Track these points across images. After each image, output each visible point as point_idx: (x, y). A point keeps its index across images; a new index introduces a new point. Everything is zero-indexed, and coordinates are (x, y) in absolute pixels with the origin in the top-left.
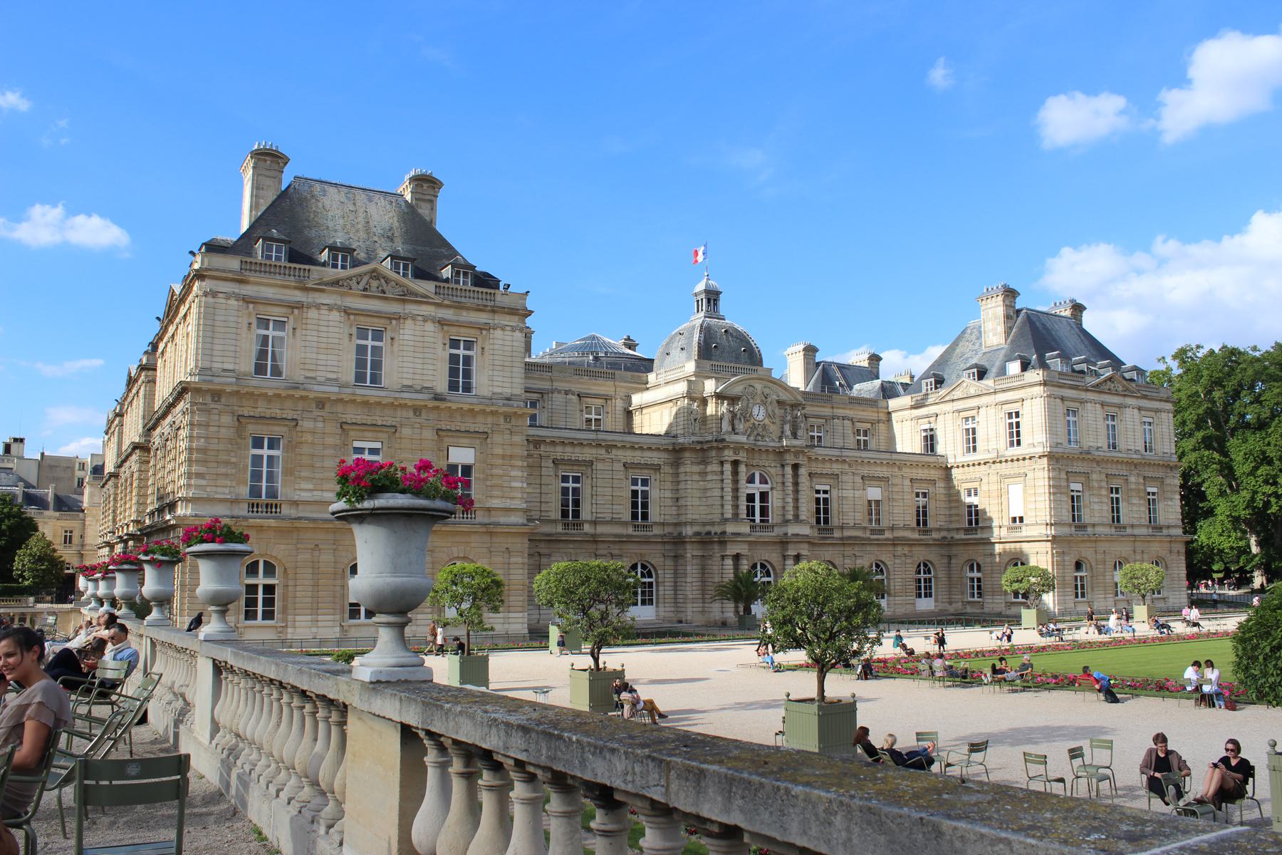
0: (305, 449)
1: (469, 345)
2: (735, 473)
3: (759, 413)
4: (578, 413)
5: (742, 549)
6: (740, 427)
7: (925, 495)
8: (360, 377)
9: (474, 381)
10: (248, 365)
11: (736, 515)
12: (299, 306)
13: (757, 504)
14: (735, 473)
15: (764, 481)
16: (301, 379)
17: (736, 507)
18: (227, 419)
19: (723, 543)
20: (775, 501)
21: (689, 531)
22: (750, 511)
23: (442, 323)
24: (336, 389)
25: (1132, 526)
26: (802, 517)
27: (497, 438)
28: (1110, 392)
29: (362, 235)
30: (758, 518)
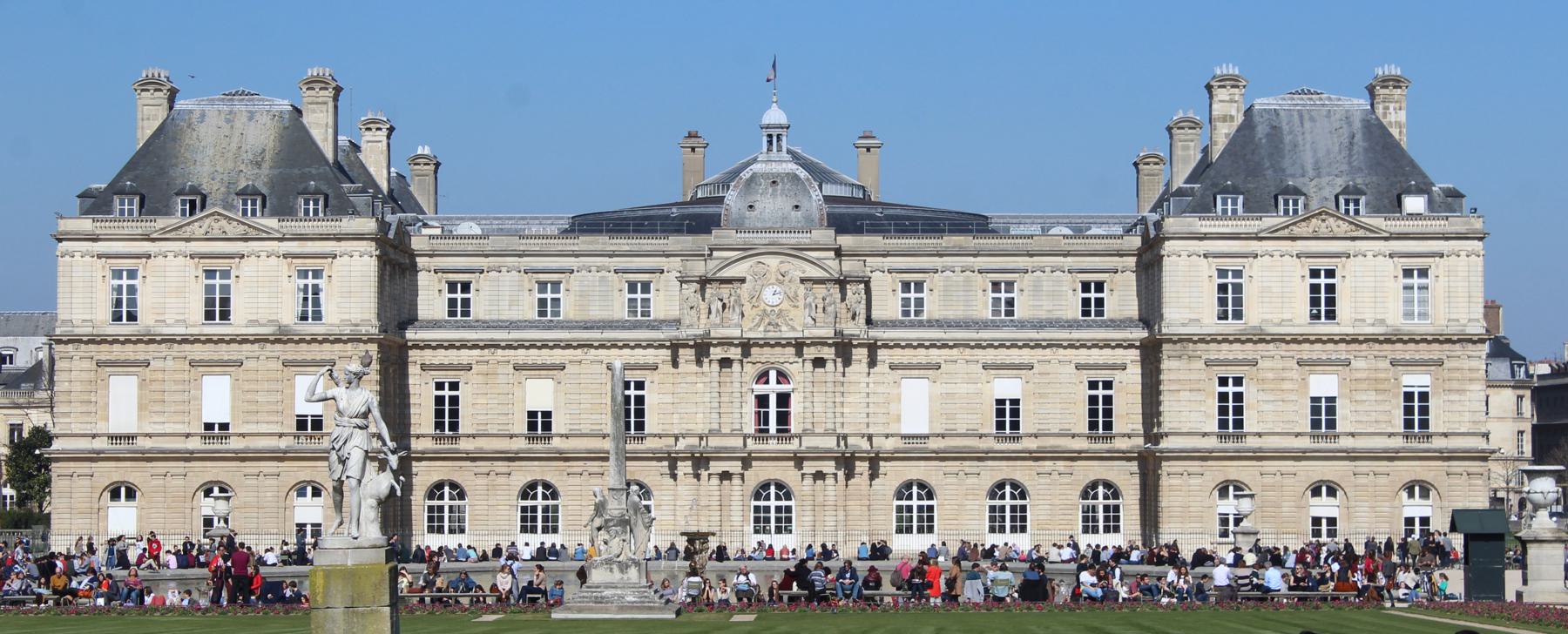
0: (156, 386)
1: (317, 274)
3: (770, 296)
4: (617, 294)
5: (735, 467)
7: (1108, 385)
8: (209, 316)
9: (323, 309)
10: (106, 312)
12: (149, 257)
13: (773, 410)
15: (782, 377)
16: (152, 323)
18: (86, 364)
19: (708, 459)
20: (795, 407)
21: (682, 444)
22: (762, 419)
23: (285, 256)
24: (182, 330)
25: (1353, 435)
29: (230, 165)
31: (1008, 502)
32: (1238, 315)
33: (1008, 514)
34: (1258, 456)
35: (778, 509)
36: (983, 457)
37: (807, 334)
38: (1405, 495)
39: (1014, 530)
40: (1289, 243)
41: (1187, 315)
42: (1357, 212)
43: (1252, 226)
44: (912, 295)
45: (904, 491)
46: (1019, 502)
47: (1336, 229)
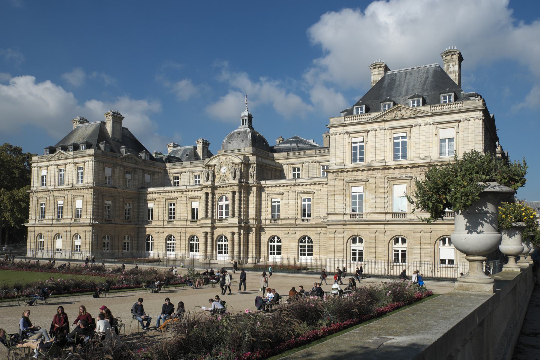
2: (207, 198)
3: (224, 170)
6: (210, 178)
11: (207, 216)
13: (224, 210)
14: (207, 198)
15: (227, 200)
17: (207, 212)
26: (237, 214)
27: (85, 196)
28: (395, 119)
30: (224, 217)
31: (306, 244)
32: (361, 160)
33: (306, 249)
34: (368, 223)
35: (225, 245)
36: (296, 226)
37: (230, 182)
38: (441, 242)
39: (308, 255)
40: (383, 123)
41: (339, 161)
42: (418, 106)
43: (367, 118)
44: (297, 172)
45: (272, 239)
46: (310, 244)
47: (405, 115)
